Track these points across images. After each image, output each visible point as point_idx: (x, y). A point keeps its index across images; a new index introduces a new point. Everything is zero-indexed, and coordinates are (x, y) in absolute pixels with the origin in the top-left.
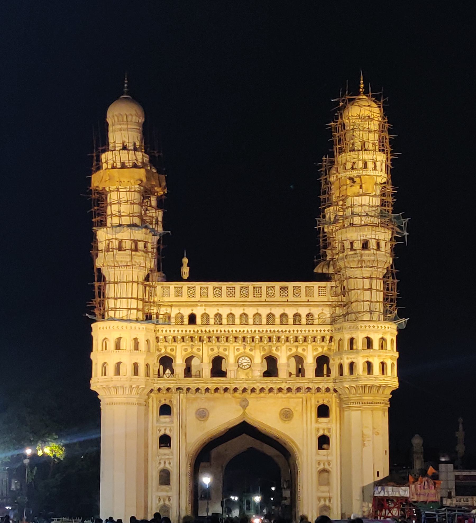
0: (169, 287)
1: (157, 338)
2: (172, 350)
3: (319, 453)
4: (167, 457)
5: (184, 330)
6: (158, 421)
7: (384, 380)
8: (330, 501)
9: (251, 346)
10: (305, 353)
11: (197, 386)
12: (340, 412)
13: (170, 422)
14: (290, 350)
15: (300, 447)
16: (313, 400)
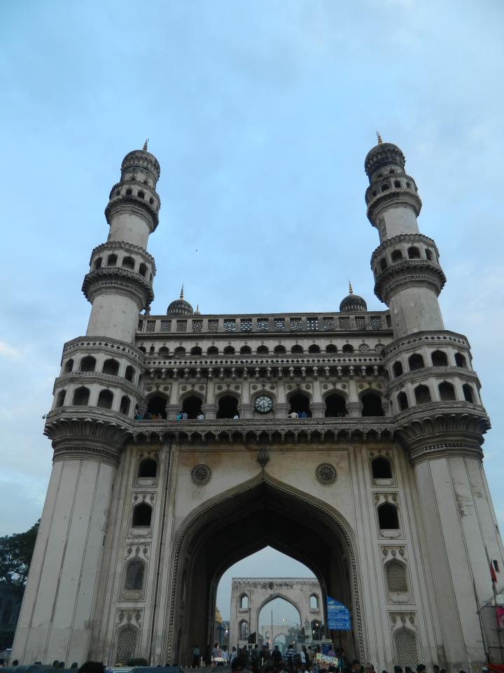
0: (171, 321)
1: (146, 373)
2: (166, 389)
3: (383, 534)
4: (142, 540)
5: (183, 361)
6: (135, 484)
7: (474, 409)
8: (412, 621)
9: (271, 383)
10: (346, 390)
11: (194, 429)
12: (408, 471)
13: (153, 484)
14: (325, 387)
15: (352, 525)
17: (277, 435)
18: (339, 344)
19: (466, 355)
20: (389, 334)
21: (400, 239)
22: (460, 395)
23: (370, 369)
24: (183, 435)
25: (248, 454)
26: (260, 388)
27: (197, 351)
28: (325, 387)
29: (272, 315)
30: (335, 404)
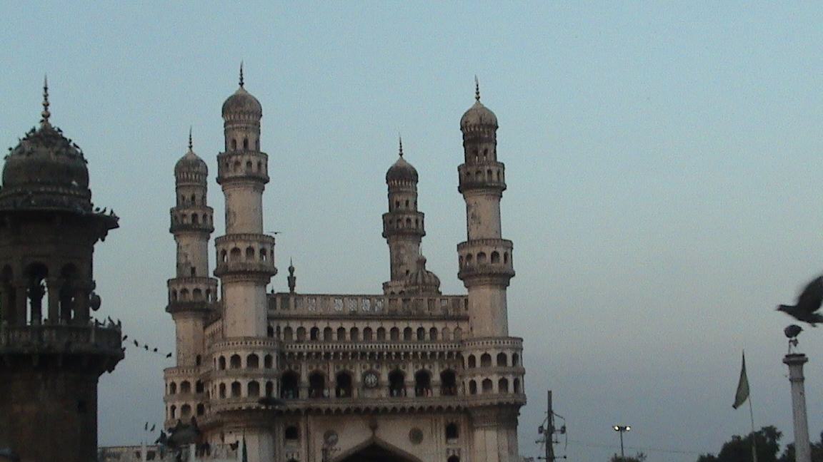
2: (296, 368)
10: (432, 370)
14: (417, 367)
16: (442, 421)
17: (385, 409)
18: (427, 326)
19: (519, 353)
20: (466, 319)
21: (485, 241)
22: (510, 362)
23: (450, 354)
24: (319, 410)
25: (362, 422)
26: (368, 367)
27: (314, 331)
28: (417, 367)
29: (373, 296)
30: (423, 380)
